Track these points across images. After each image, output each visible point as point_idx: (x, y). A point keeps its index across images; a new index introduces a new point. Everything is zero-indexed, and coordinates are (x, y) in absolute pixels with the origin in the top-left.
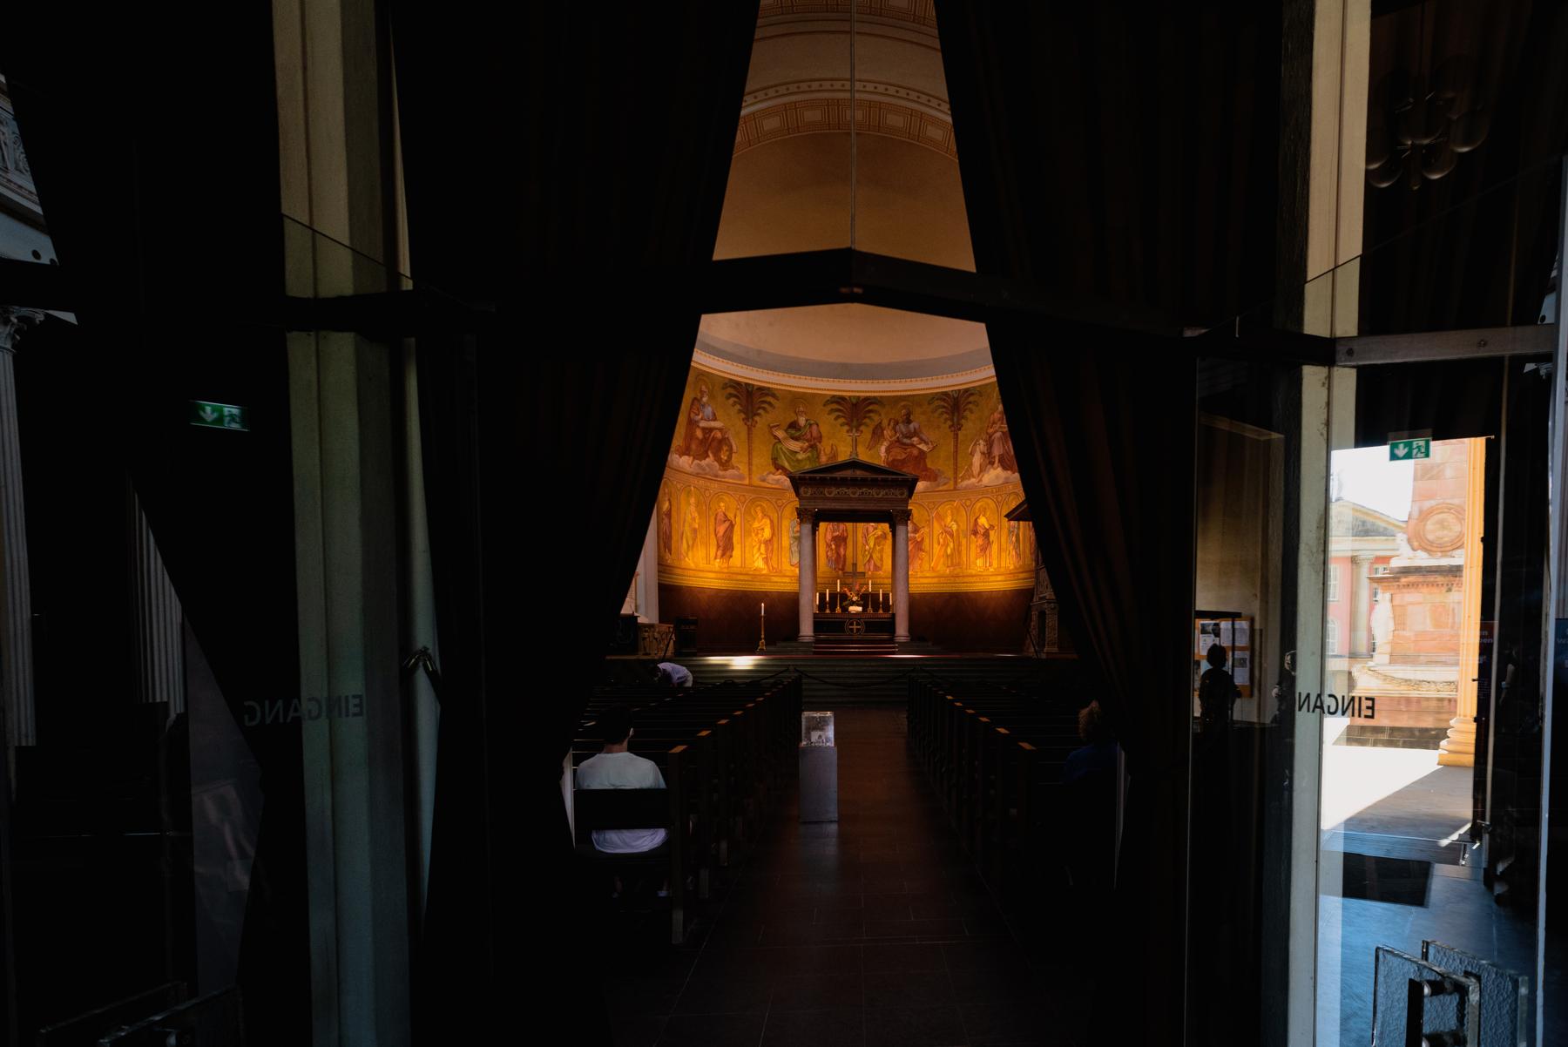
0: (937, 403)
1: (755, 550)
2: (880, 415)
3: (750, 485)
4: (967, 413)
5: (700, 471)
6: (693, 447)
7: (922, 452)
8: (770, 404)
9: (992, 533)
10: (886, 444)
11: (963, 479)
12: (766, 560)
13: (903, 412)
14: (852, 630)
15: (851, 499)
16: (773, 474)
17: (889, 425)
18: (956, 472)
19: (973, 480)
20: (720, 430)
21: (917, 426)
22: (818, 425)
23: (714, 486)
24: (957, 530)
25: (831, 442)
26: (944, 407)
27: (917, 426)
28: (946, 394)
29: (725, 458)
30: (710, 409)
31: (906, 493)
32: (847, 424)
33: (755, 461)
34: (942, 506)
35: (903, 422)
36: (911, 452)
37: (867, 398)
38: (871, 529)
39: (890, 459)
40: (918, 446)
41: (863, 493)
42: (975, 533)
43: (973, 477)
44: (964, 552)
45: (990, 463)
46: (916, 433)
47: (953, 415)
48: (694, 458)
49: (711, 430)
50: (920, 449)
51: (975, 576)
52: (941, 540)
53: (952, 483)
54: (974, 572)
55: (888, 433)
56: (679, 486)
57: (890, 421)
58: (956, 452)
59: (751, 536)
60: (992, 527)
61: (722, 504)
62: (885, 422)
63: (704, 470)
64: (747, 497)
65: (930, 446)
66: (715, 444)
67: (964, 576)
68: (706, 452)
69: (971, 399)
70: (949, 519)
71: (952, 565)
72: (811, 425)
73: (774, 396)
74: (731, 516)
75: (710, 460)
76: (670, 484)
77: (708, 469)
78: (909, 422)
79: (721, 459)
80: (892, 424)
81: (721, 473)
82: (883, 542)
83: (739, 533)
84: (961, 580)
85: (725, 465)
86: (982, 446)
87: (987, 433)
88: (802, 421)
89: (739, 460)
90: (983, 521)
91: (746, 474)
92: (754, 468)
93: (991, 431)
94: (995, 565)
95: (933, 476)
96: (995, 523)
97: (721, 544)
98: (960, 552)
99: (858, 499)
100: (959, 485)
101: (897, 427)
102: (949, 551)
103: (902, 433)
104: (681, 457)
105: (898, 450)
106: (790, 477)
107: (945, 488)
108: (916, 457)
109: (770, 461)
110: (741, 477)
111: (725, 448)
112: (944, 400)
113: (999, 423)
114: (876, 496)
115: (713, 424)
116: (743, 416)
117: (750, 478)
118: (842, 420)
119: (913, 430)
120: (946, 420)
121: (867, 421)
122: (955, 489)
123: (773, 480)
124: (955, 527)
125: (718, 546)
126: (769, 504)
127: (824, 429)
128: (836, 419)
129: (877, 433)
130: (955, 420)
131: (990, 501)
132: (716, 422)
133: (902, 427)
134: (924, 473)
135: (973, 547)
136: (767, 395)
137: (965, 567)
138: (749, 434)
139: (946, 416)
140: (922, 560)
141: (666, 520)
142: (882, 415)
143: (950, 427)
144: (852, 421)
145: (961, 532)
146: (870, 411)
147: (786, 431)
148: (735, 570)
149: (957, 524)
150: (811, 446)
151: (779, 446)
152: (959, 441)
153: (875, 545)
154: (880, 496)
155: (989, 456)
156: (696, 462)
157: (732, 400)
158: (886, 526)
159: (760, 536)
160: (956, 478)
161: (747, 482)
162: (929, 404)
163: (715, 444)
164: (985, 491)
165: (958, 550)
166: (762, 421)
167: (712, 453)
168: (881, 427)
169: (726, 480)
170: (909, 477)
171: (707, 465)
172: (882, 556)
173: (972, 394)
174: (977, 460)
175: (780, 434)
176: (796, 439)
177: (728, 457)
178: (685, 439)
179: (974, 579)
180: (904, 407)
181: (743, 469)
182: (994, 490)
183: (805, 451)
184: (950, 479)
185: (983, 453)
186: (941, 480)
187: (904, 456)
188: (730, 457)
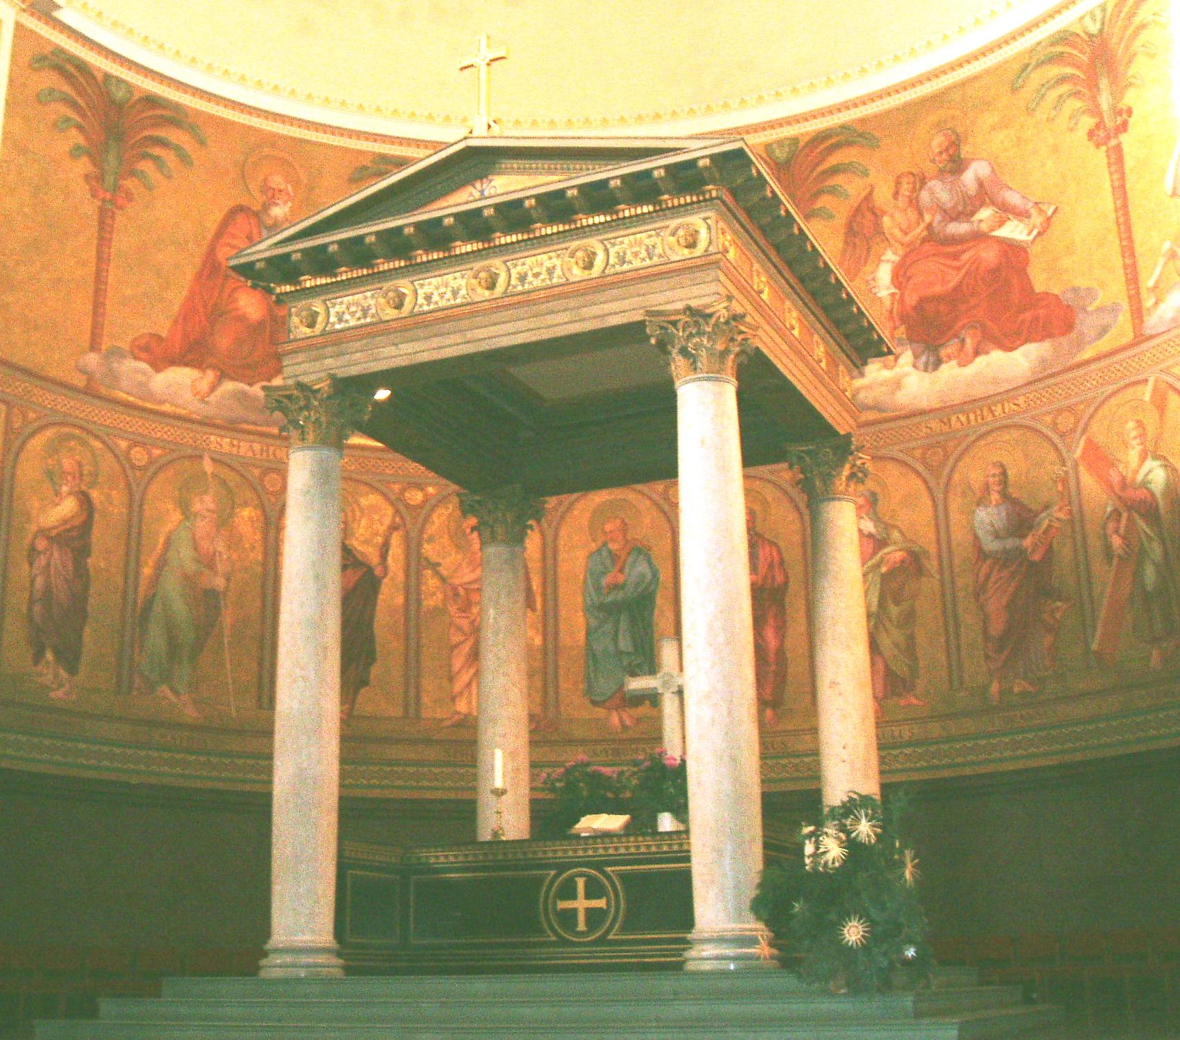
5: (252, 417)
6: (223, 341)
14: (594, 890)
17: (896, 195)
35: (941, 171)
39: (911, 300)
40: (998, 233)
47: (1093, 85)
50: (1001, 241)
52: (1116, 541)
53: (1124, 319)
57: (898, 183)
65: (1037, 219)
101: (925, 196)
102: (1150, 575)
104: (158, 370)
105: (931, 265)
107: (1104, 345)
108: (995, 271)
112: (1058, 59)
122: (1140, 338)
134: (1028, 315)
139: (1074, 104)
142: (873, 172)
143: (1091, 134)
146: (834, 171)
152: (1129, 162)
168: (872, 210)
172: (911, 637)
186: (1086, 324)
187: (954, 279)
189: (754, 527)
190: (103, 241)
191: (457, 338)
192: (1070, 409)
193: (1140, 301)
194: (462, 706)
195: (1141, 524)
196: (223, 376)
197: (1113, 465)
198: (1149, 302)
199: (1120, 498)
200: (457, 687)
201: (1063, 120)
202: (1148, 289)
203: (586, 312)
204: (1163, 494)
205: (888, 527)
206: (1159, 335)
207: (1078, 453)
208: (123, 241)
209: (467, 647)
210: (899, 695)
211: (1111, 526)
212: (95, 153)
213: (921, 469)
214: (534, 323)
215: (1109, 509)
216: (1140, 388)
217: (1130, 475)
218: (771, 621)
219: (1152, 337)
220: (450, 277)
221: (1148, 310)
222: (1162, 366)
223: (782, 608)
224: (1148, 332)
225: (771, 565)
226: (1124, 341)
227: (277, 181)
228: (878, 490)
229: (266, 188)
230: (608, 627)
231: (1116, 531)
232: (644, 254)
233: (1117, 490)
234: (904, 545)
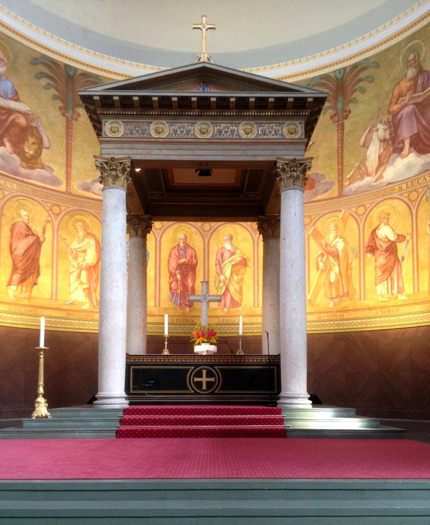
1: (73, 277)
3: (68, 193)
9: (401, 247)
11: (352, 180)
12: (89, 292)
15: (197, 142)
18: (341, 173)
19: (368, 180)
20: (24, 114)
24: (345, 250)
28: (325, 77)
29: (31, 152)
30: (9, 85)
34: (322, 219)
38: (227, 255)
41: (220, 132)
45: (395, 151)
51: (374, 308)
52: (321, 265)
54: (371, 303)
59: (68, 259)
60: (401, 238)
61: (23, 213)
64: (63, 208)
66: (14, 131)
70: (332, 236)
71: (337, 297)
79: (24, 152)
82: (242, 270)
83: (50, 253)
84: (346, 315)
91: (62, 176)
94: (409, 289)
96: (406, 230)
97: (20, 265)
99: (208, 142)
106: (144, 237)
110: (56, 181)
111: (31, 140)
114: (244, 136)
115: (13, 105)
116: (61, 104)
124: (340, 245)
125: (15, 269)
126: (95, 219)
130: (339, 106)
131: (396, 203)
132: (17, 103)
137: (357, 296)
145: (349, 250)
148: (42, 303)
153: (231, 275)
154: (252, 136)
155: (393, 142)
157: (44, 82)
159: (80, 259)
161: (63, 188)
169: (32, 181)
172: (241, 288)
173: (364, 69)
177: (36, 152)
179: (373, 313)
182: (404, 186)
188: (38, 153)
189: (186, 241)
191: (190, 152)
193: (342, 183)
195: (331, 259)
197: (323, 238)
199: (324, 250)
202: (347, 179)
203: (249, 153)
204: (342, 250)
205: (236, 248)
206: (348, 195)
207: (310, 232)
210: (236, 307)
211: (320, 259)
213: (249, 229)
214: (224, 153)
215: (320, 253)
216: (338, 213)
217: (329, 243)
218: (190, 276)
219: (345, 196)
220: (186, 125)
221: (346, 186)
222: (348, 207)
223: (195, 273)
224: (344, 193)
225: (191, 257)
226: (334, 196)
228: (233, 234)
231: (322, 260)
232: (273, 133)
233: (324, 247)
234: (241, 256)
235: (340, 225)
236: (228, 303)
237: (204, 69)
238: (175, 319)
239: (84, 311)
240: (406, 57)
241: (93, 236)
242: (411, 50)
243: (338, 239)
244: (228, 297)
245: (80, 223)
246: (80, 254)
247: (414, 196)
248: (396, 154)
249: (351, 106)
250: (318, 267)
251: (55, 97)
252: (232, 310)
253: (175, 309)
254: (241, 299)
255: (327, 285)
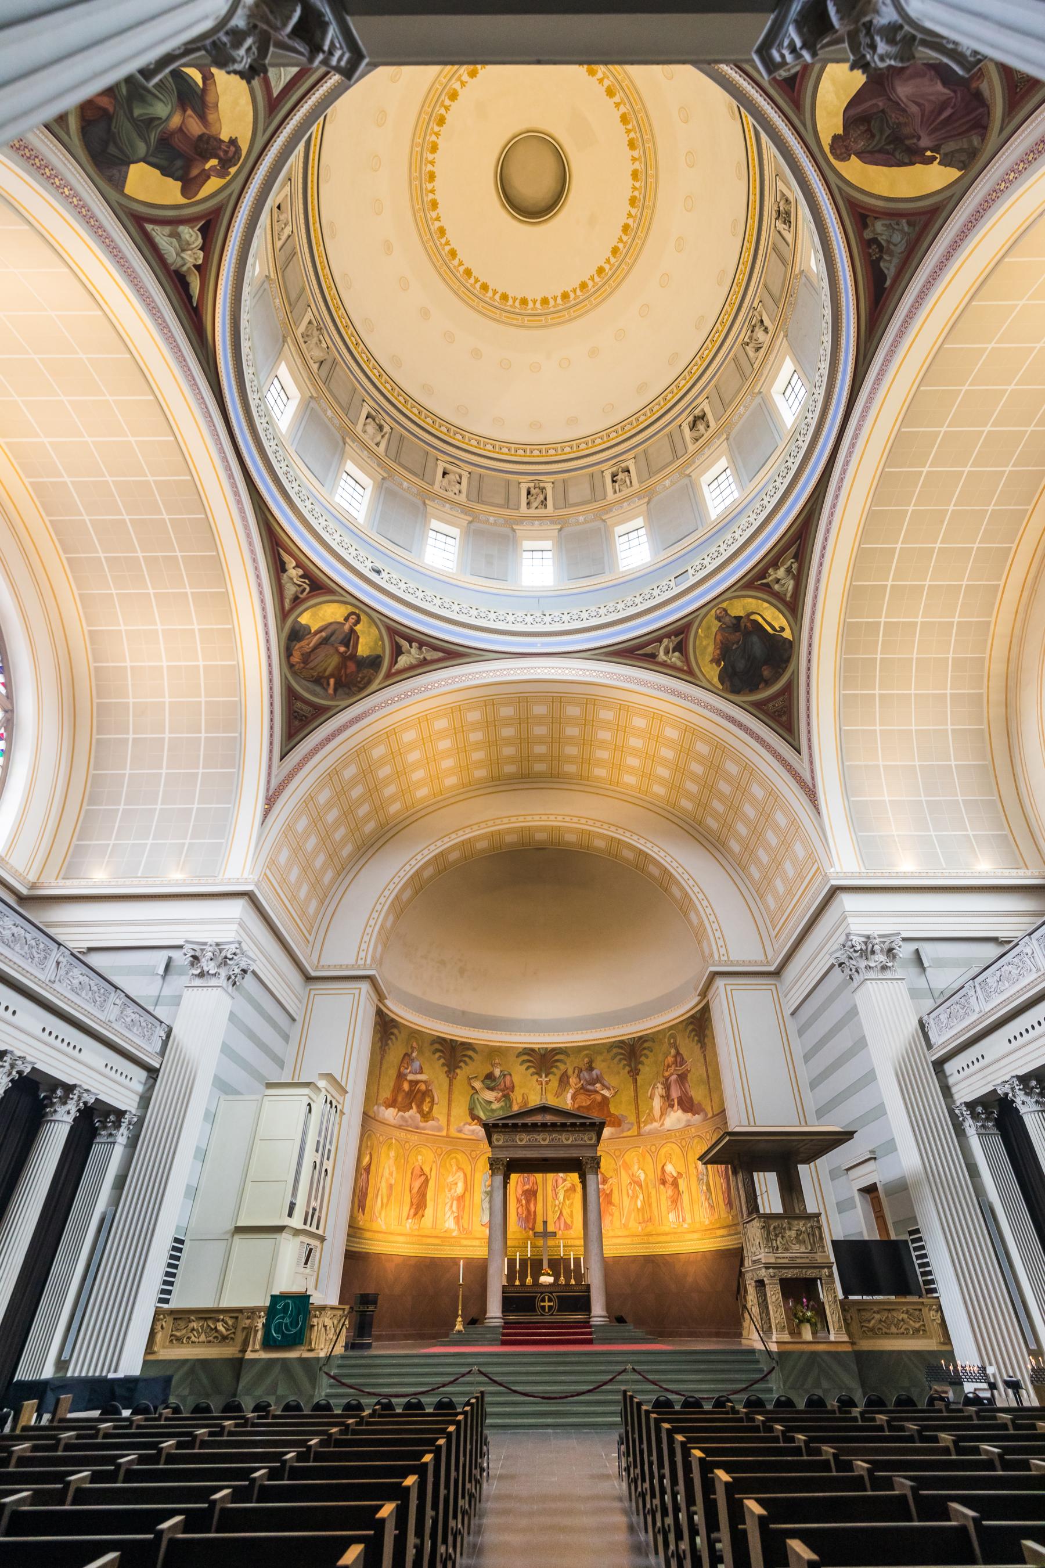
0: (615, 1050)
2: (565, 1064)
4: (643, 1059)
5: (404, 1124)
6: (400, 1099)
7: (604, 1097)
8: (470, 1058)
9: (680, 1181)
10: (571, 1091)
11: (646, 1123)
13: (586, 1060)
16: (470, 1124)
18: (638, 1117)
19: (655, 1125)
20: (425, 1082)
21: (599, 1073)
22: (511, 1075)
23: (414, 1138)
24: (645, 1179)
25: (522, 1091)
26: (622, 1054)
27: (599, 1073)
28: (622, 1042)
31: (594, 1138)
32: (537, 1073)
33: (454, 1112)
36: (594, 1101)
37: (554, 1049)
38: (560, 1181)
39: (576, 1106)
42: (663, 1182)
43: (656, 1121)
44: (654, 1205)
46: (598, 1080)
47: (631, 1061)
48: (399, 1110)
49: (417, 1082)
50: (603, 1095)
51: (667, 1234)
52: (630, 1192)
53: (635, 1127)
55: (573, 1080)
56: (381, 1139)
57: (574, 1069)
58: (636, 1097)
61: (420, 1157)
62: (570, 1072)
63: (407, 1121)
65: (612, 1092)
66: (419, 1095)
67: (658, 1235)
68: (411, 1104)
69: (646, 1045)
70: (636, 1167)
71: (644, 1222)
72: (505, 1075)
73: (474, 1050)
74: (426, 1169)
75: (413, 1111)
76: (373, 1136)
77: (410, 1120)
78: (591, 1069)
80: (576, 1072)
81: (422, 1125)
82: (572, 1196)
84: (651, 1239)
85: (426, 1116)
86: (660, 1090)
87: (663, 1077)
88: (497, 1072)
89: (439, 1111)
90: (669, 1168)
92: (452, 1119)
93: (667, 1074)
94: (689, 1220)
95: (617, 1122)
98: (650, 1205)
100: (642, 1131)
103: (586, 1080)
105: (583, 1097)
107: (629, 1133)
108: (600, 1103)
109: (468, 1112)
110: (440, 1129)
111: (428, 1100)
112: (621, 1048)
113: (673, 1066)
115: (419, 1077)
116: (446, 1069)
117: (448, 1130)
118: (532, 1070)
119: (595, 1076)
120: (625, 1066)
121: (554, 1070)
123: (469, 1130)
124: (642, 1177)
126: (464, 1156)
127: (516, 1079)
128: (528, 1068)
129: (564, 1080)
131: (674, 1146)
133: (585, 1075)
135: (663, 1198)
136: (468, 1049)
137: (657, 1223)
138: (450, 1085)
140: (612, 1215)
141: (364, 1176)
143: (629, 1072)
144: (541, 1070)
146: (557, 1061)
147: (482, 1082)
149: (645, 1173)
150: (504, 1096)
151: (476, 1096)
152: (638, 1084)
156: (401, 1113)
158: (574, 1177)
160: (638, 1123)
161: (444, 1133)
162: (608, 1052)
163: (419, 1095)
164: (667, 1136)
165: (647, 1203)
166: (462, 1074)
167: (416, 1104)
170: (597, 1120)
171: (410, 1117)
173: (646, 1041)
174: (657, 1103)
175: (477, 1085)
176: (491, 1089)
178: (393, 1091)
179: (668, 1238)
180: (587, 1055)
181: (443, 1121)
183: (498, 1100)
184: (632, 1124)
185: (662, 1097)
186: (625, 1126)
188: (431, 1109)
190: (381, 1068)
192: (619, 1149)
194: (447, 1225)
195: (637, 1188)
196: (399, 1110)
198: (642, 1125)
200: (447, 1216)
201: (621, 1065)
208: (384, 1067)
209: (449, 1204)
212: (381, 1039)
227: (415, 1045)
229: (412, 1047)
230: (488, 1199)
235: (641, 1159)
236: (562, 1227)
237: (544, 1107)
238: (521, 1241)
239: (454, 1237)
240: (669, 1040)
241: (463, 1170)
242: (672, 1036)
243: (640, 1171)
244: (562, 1221)
245: (454, 1160)
246: (453, 1186)
247: (684, 1143)
248: (669, 1109)
249: (640, 1067)
250: (628, 1194)
251: (443, 1065)
252: (565, 1232)
253: (521, 1232)
254: (572, 1222)
255: (636, 1210)
